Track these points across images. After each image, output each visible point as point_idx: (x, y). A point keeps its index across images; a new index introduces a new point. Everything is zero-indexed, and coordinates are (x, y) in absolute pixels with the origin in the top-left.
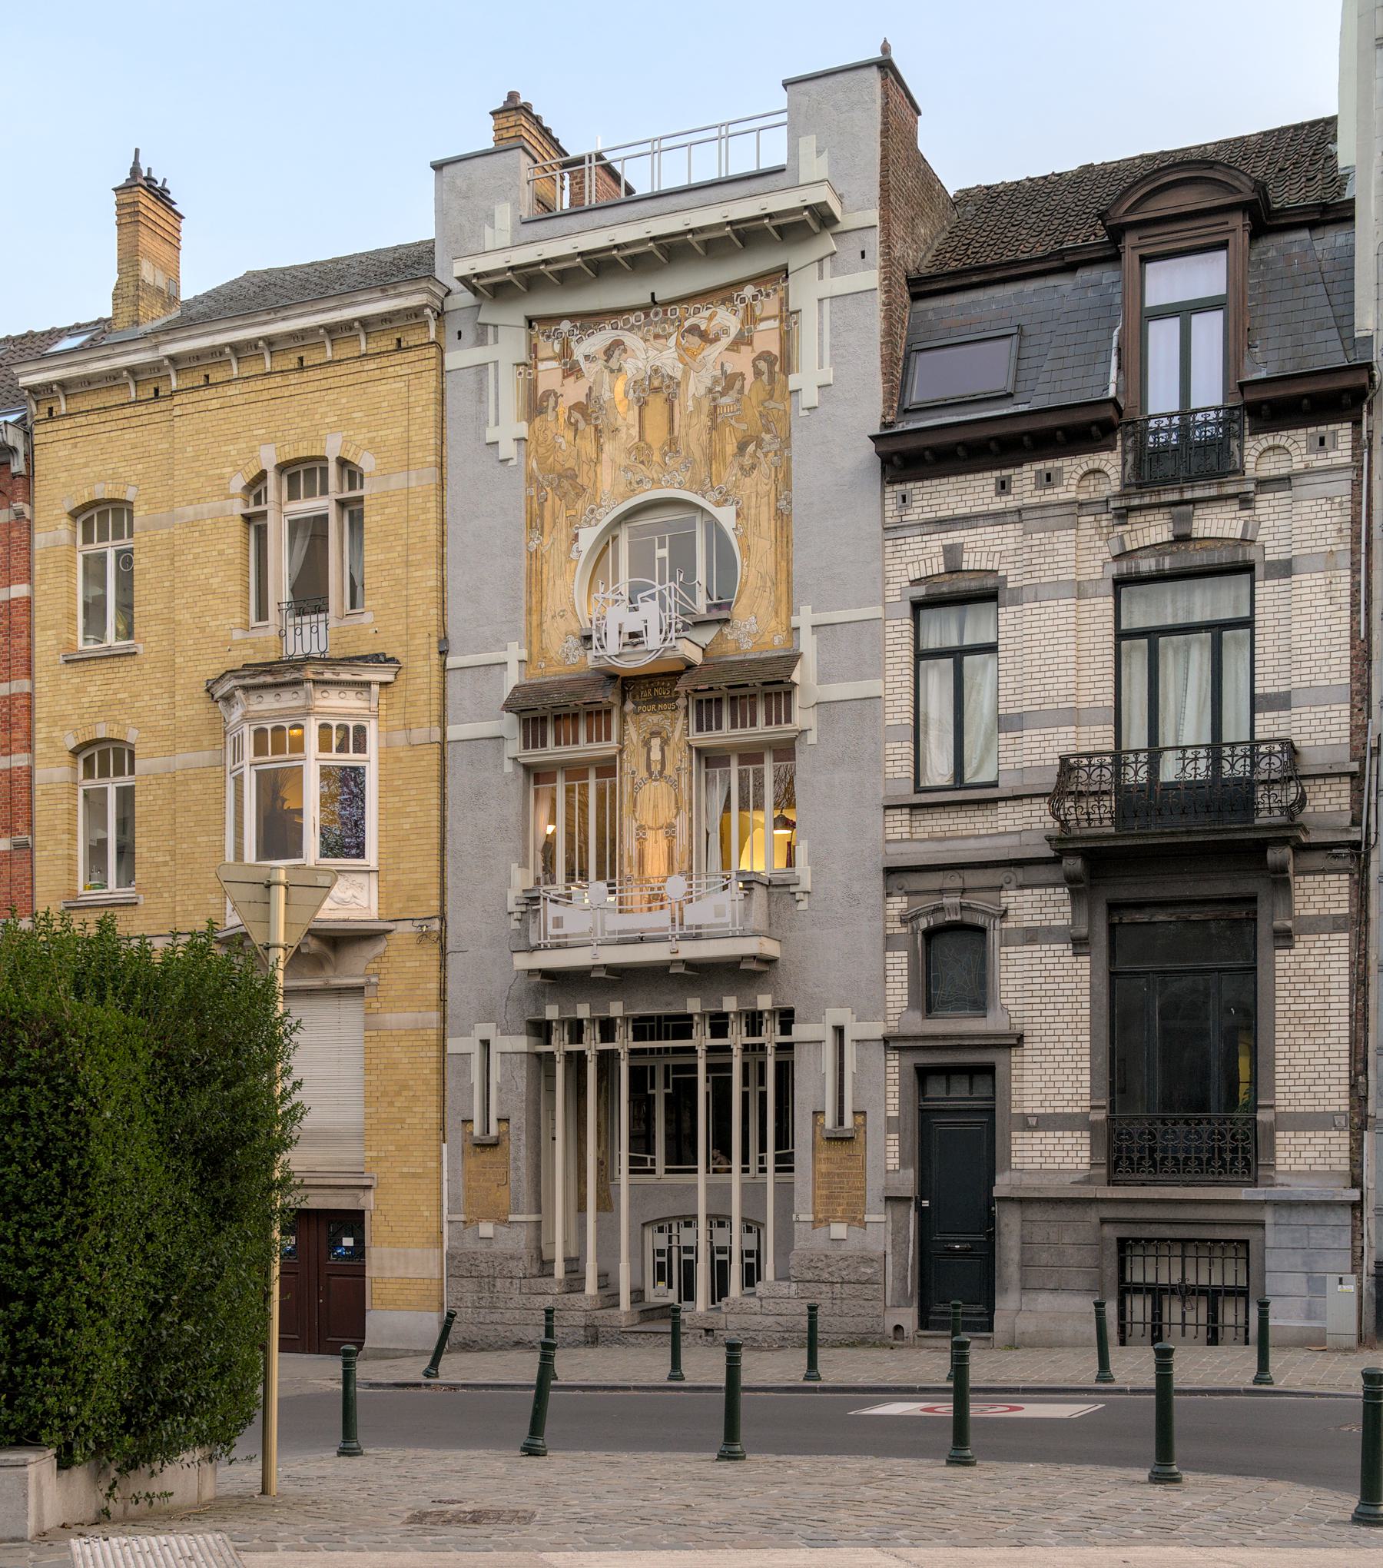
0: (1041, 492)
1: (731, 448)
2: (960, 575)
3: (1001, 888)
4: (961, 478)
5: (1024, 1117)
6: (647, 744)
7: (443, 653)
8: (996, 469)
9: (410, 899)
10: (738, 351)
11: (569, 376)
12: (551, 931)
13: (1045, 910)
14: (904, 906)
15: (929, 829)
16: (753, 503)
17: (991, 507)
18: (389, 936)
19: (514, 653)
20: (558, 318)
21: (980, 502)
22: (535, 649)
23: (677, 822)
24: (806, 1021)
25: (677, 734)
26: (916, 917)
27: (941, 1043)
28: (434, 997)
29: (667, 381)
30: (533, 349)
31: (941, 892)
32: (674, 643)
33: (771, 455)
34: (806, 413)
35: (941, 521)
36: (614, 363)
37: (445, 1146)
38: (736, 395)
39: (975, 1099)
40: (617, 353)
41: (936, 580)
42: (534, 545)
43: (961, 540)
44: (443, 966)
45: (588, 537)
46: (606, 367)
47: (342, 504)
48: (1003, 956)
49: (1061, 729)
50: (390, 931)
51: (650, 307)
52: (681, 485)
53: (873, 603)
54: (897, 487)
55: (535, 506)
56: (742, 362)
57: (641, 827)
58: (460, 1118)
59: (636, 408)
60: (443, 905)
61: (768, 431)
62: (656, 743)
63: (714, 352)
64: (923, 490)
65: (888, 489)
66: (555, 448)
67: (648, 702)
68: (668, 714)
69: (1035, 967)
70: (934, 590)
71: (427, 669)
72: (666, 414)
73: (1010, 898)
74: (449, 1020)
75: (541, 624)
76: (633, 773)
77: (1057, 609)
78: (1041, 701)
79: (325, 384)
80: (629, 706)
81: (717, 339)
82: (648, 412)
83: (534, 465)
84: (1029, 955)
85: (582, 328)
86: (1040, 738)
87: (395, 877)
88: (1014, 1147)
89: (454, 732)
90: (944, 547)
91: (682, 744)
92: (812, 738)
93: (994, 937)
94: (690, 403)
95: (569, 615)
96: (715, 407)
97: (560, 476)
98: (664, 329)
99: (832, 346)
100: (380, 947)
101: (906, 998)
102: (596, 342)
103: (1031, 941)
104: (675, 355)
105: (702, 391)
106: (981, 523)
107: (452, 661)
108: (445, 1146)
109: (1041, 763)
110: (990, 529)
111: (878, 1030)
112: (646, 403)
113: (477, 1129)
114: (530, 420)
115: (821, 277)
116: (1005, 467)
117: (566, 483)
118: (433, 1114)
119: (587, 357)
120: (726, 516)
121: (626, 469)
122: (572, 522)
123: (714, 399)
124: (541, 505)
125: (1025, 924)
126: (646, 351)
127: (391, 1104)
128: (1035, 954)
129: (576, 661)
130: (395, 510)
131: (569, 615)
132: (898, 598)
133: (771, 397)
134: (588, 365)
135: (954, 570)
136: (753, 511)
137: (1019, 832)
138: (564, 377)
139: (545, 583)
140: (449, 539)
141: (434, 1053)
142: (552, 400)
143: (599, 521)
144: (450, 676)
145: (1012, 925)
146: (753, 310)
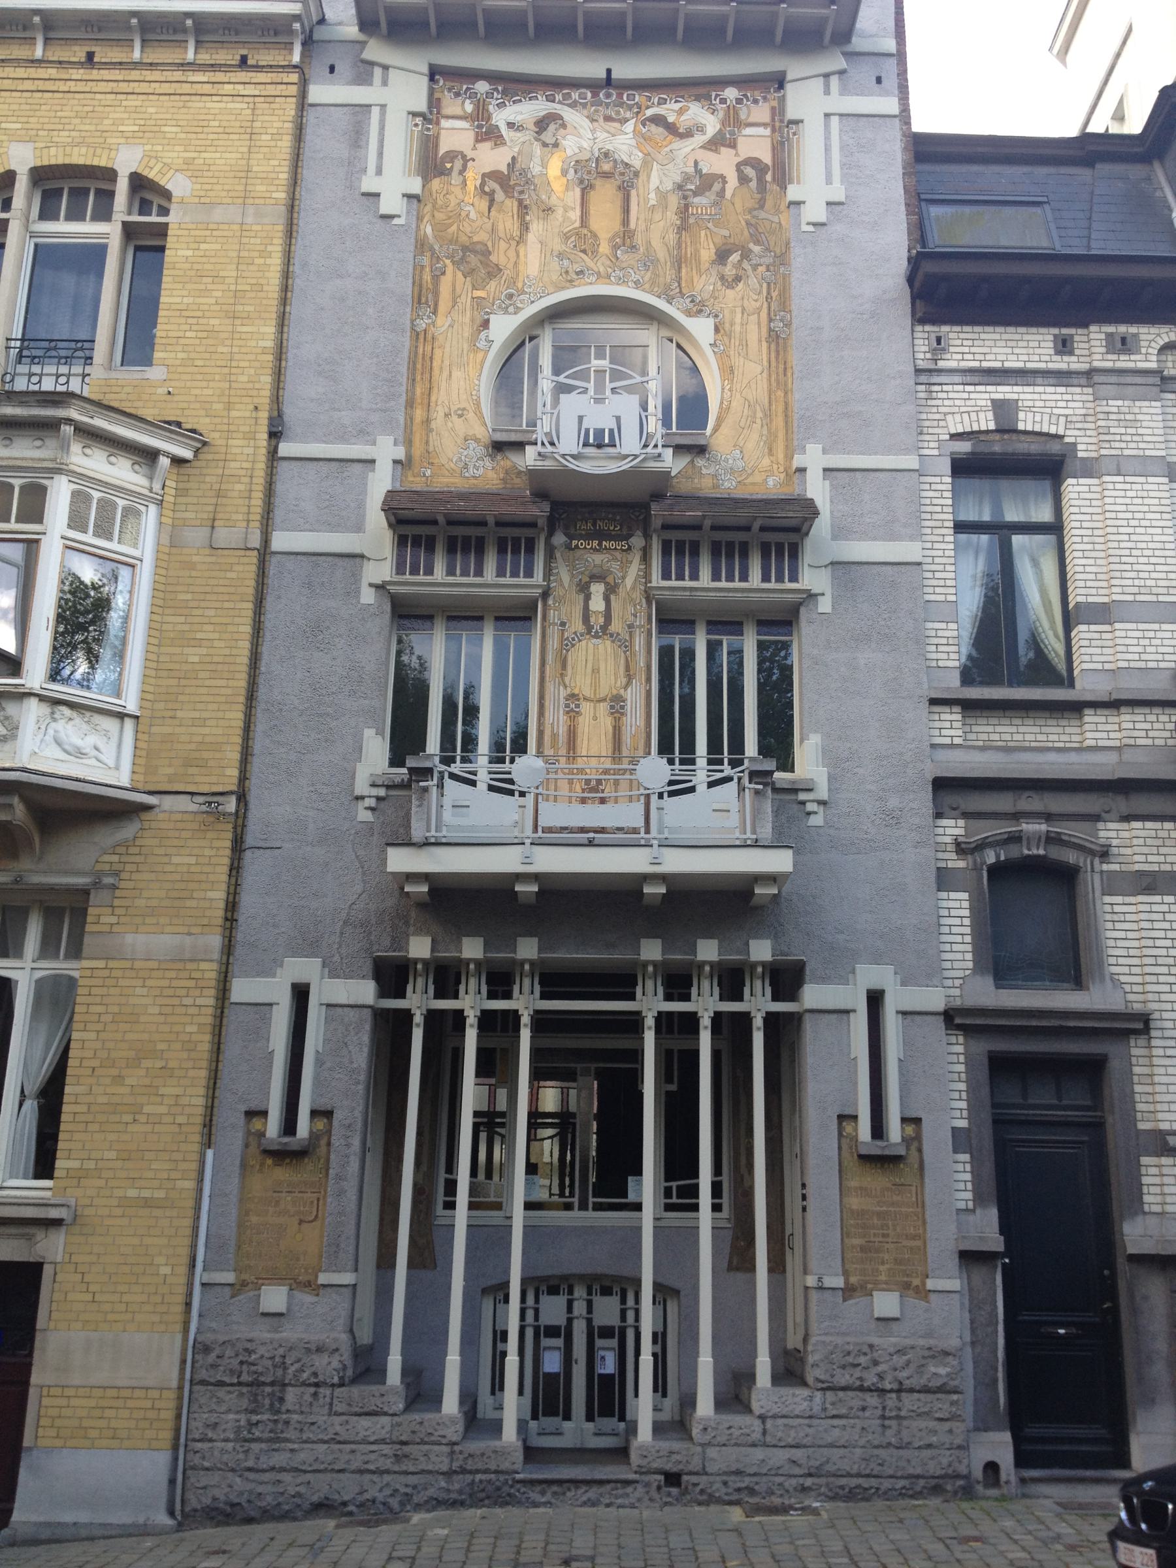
0: (1115, 357)
1: (707, 254)
2: (1014, 437)
3: (1096, 818)
4: (1011, 329)
5: (1161, 1135)
6: (584, 589)
7: (275, 435)
8: (1054, 325)
9: (188, 763)
10: (716, 151)
11: (483, 140)
12: (447, 815)
13: (1163, 850)
14: (961, 832)
15: (985, 737)
16: (738, 319)
17: (1051, 366)
18: (145, 816)
19: (386, 450)
20: (474, 75)
21: (1037, 358)
22: (417, 450)
23: (628, 695)
24: (824, 980)
25: (629, 582)
26: (981, 846)
27: (1034, 1023)
28: (218, 913)
29: (621, 168)
30: (434, 102)
31: (1016, 816)
32: (659, 450)
33: (760, 268)
34: (811, 228)
35: (990, 372)
36: (548, 137)
37: (210, 1153)
38: (713, 197)
39: (1066, 1108)
40: (552, 127)
41: (982, 437)
42: (422, 324)
43: (1015, 396)
44: (235, 869)
45: (503, 327)
46: (537, 140)
47: (129, 231)
48: (1108, 908)
49: (1165, 627)
50: (148, 808)
51: (601, 87)
52: (638, 285)
53: (906, 451)
54: (928, 328)
55: (427, 277)
56: (723, 163)
57: (573, 696)
58: (244, 1108)
59: (578, 191)
60: (243, 778)
61: (757, 242)
62: (597, 589)
63: (686, 149)
64: (962, 336)
65: (919, 328)
66: (457, 216)
67: (589, 537)
68: (618, 554)
69: (1157, 925)
70: (982, 448)
71: (251, 451)
72: (619, 203)
73: (1111, 832)
74: (239, 951)
75: (427, 421)
76: (563, 624)
77: (1146, 487)
78: (1136, 590)
79: (124, 87)
80: (559, 539)
81: (688, 134)
82: (593, 196)
83: (429, 230)
84: (1147, 908)
85: (505, 93)
86: (1140, 634)
87: (167, 730)
88: (1145, 1180)
89: (281, 541)
90: (993, 401)
91: (638, 595)
92: (825, 605)
93: (1092, 881)
94: (652, 196)
95: (471, 415)
96: (686, 207)
97: (465, 249)
98: (618, 113)
99: (843, 165)
100: (128, 830)
101: (969, 956)
102: (527, 110)
103: (1150, 890)
104: (633, 142)
105: (669, 185)
106: (1039, 380)
107: (285, 449)
108: (210, 1153)
109: (1142, 665)
110: (1051, 389)
111: (934, 999)
112: (592, 187)
113: (273, 1126)
114: (426, 180)
115: (827, 92)
116: (1066, 326)
117: (473, 259)
118: (197, 1100)
119: (511, 125)
120: (701, 329)
121: (561, 256)
122: (478, 302)
123: (685, 198)
124: (436, 279)
125: (1137, 867)
126: (593, 131)
127: (119, 1079)
128: (1155, 908)
129: (477, 473)
130: (218, 247)
131: (471, 415)
132: (936, 452)
133: (762, 207)
134: (512, 133)
135: (1006, 428)
136: (737, 328)
137: (1118, 749)
138: (477, 141)
139: (436, 372)
140: (295, 298)
141: (208, 1000)
142: (458, 164)
143: (518, 310)
144: (283, 467)
145: (1116, 867)
146: (736, 113)
